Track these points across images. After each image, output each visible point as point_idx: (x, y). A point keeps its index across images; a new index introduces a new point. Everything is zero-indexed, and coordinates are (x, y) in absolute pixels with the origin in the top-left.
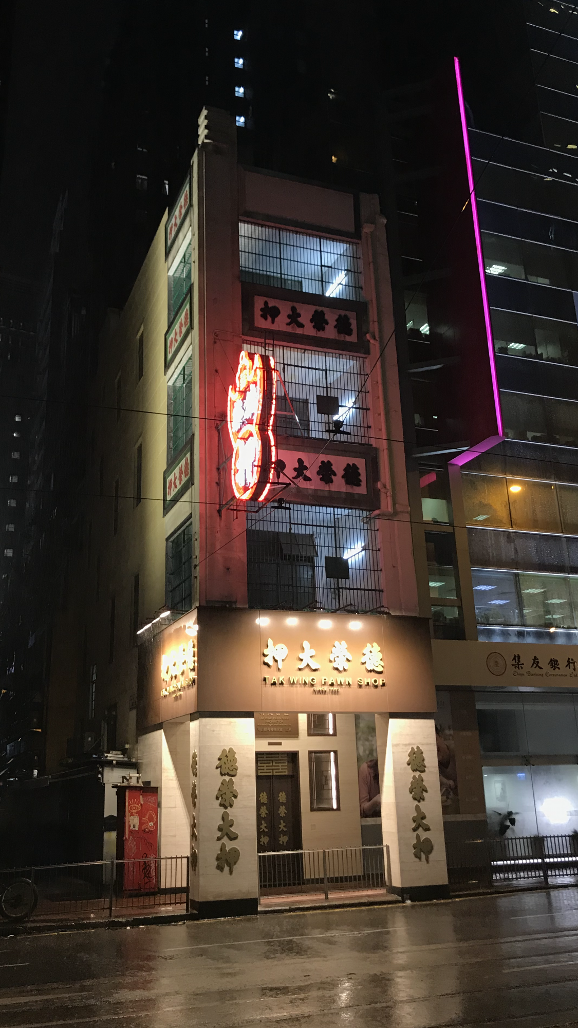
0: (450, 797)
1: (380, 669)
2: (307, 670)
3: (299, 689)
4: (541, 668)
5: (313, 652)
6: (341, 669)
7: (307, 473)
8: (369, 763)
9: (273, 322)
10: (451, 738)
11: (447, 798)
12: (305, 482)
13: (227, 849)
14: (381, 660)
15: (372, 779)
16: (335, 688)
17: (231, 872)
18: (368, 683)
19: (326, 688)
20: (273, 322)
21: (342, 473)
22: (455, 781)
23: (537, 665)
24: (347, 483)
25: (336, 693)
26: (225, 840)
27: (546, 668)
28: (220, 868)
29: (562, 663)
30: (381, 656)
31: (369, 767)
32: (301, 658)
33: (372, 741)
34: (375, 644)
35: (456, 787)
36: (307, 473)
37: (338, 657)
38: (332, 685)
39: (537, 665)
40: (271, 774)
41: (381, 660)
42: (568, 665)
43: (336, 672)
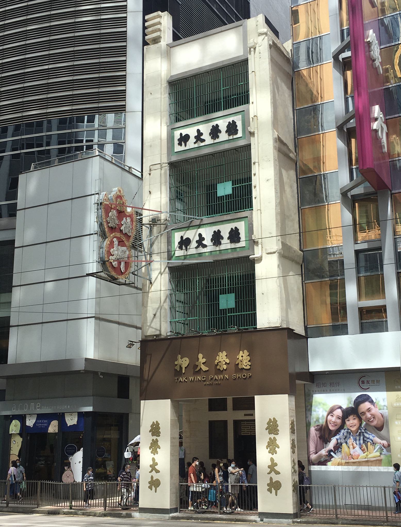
0: (383, 453)
1: (248, 367)
5: (204, 360)
7: (204, 242)
8: (316, 428)
9: (185, 145)
10: (385, 408)
11: (381, 454)
12: (203, 249)
14: (249, 361)
15: (318, 438)
18: (239, 377)
20: (185, 145)
21: (228, 235)
22: (388, 441)
24: (231, 242)
30: (249, 358)
31: (316, 430)
33: (318, 412)
34: (245, 351)
35: (389, 445)
36: (204, 242)
40: (250, 434)
41: (249, 361)
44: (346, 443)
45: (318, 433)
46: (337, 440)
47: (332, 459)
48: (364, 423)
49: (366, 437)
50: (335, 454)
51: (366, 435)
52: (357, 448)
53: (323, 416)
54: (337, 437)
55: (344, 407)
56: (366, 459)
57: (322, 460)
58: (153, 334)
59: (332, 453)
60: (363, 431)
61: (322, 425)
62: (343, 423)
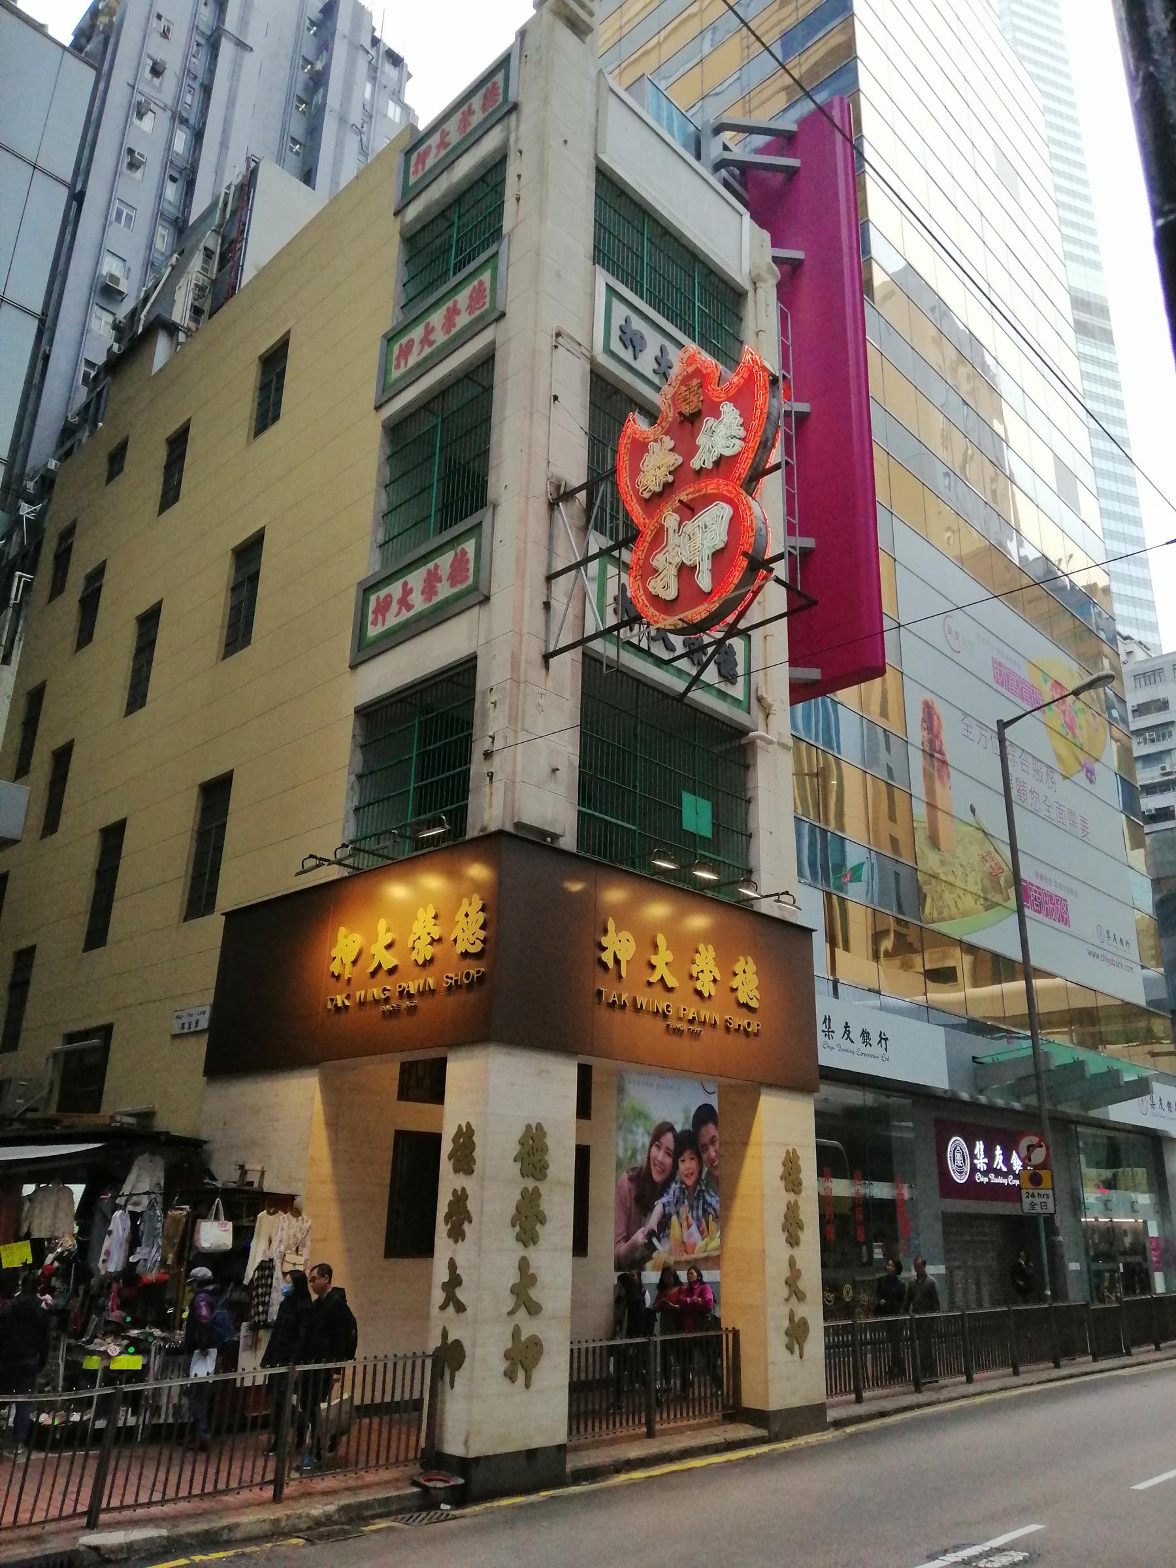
2: (659, 988)
3: (647, 1021)
4: (852, 1042)
6: (706, 995)
13: (523, 1339)
16: (696, 1028)
17: (527, 1386)
19: (684, 1026)
23: (848, 1037)
25: (695, 1035)
26: (522, 1313)
27: (858, 1040)
28: (510, 1375)
29: (875, 1038)
31: (631, 1179)
32: (654, 963)
37: (702, 971)
38: (692, 1021)
39: (848, 1037)
42: (880, 1042)
43: (697, 998)
44: (678, 1213)
45: (632, 1186)
46: (664, 1206)
47: (654, 1255)
48: (706, 1169)
49: (708, 1203)
50: (659, 1241)
51: (708, 1198)
52: (694, 1228)
53: (643, 1146)
54: (664, 1200)
55: (678, 1128)
56: (705, 1255)
57: (638, 1255)
58: (547, 828)
59: (655, 1240)
60: (703, 1188)
61: (641, 1168)
62: (675, 1167)
